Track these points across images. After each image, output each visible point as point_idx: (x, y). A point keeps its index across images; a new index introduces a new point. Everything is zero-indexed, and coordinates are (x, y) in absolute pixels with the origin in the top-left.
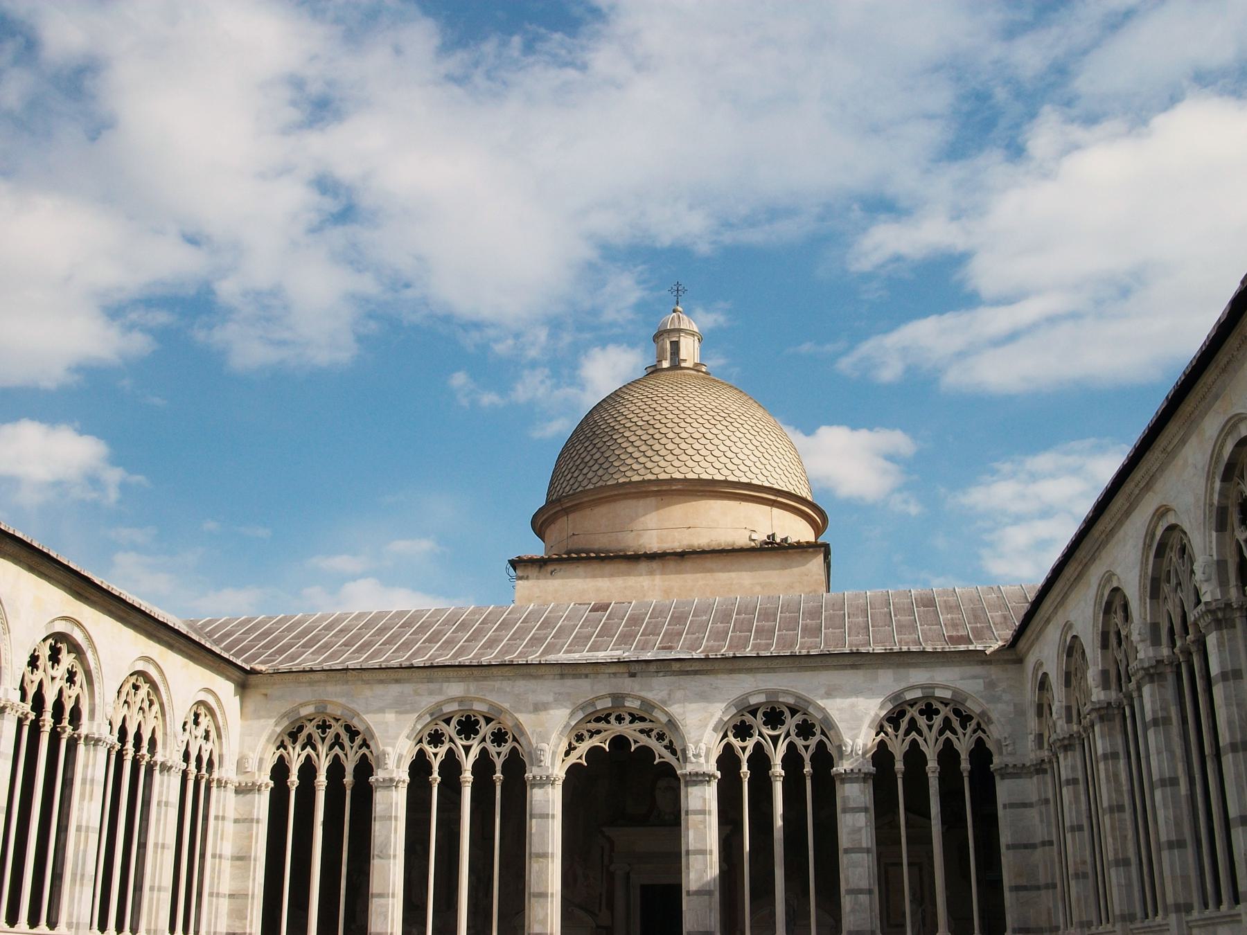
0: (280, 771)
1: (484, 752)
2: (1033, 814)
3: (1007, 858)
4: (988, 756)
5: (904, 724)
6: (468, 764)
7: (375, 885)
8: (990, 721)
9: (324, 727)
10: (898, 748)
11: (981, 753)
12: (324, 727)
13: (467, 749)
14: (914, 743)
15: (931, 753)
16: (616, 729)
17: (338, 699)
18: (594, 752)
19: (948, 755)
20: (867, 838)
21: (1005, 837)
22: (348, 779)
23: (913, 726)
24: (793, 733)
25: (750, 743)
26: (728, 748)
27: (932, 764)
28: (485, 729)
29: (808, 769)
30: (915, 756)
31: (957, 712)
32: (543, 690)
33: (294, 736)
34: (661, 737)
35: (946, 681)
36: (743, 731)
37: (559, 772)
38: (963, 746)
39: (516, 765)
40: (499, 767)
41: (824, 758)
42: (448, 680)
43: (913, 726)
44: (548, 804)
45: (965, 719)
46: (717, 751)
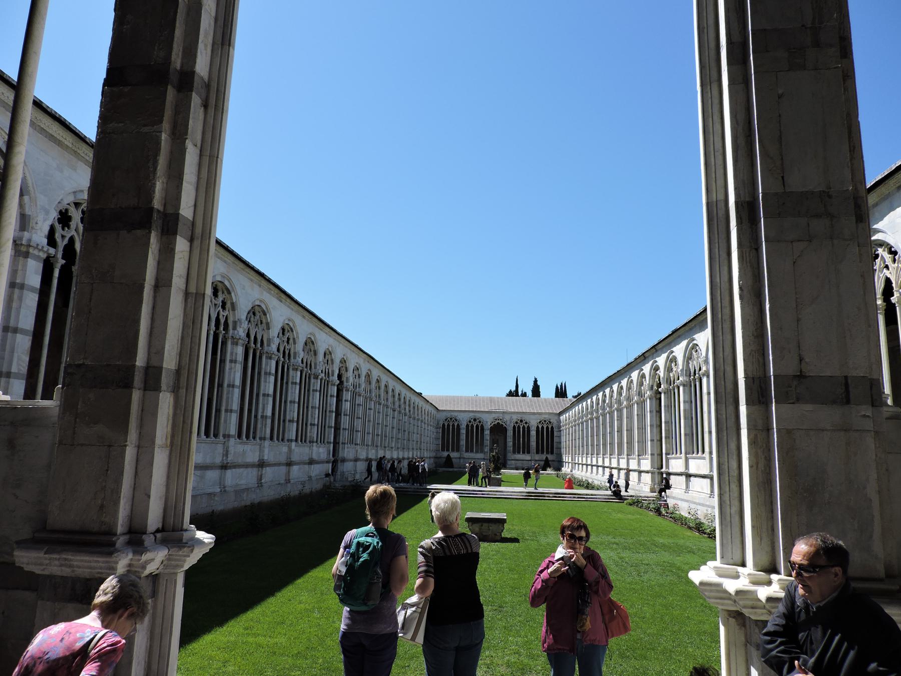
0: (444, 425)
11: (552, 428)
19: (547, 428)
30: (543, 428)
39: (482, 426)
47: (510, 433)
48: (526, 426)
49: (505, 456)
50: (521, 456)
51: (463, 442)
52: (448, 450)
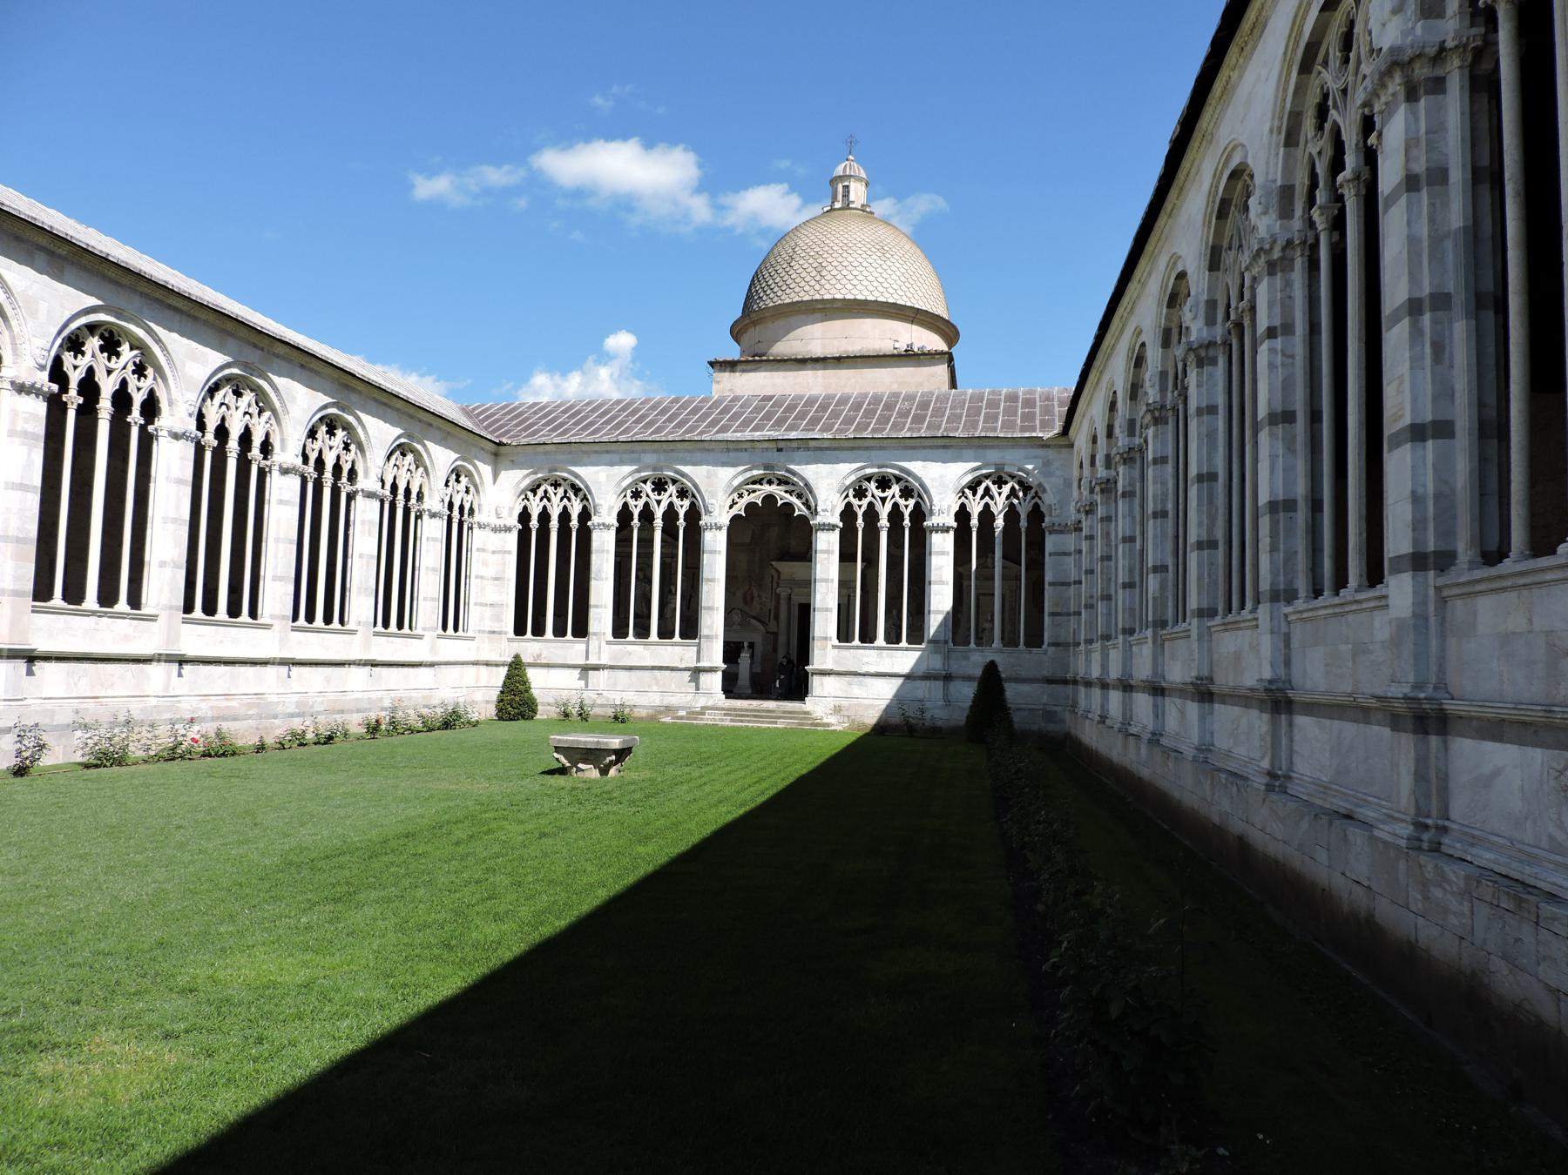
0: (524, 517)
1: (671, 505)
2: (1071, 560)
4: (1042, 517)
5: (981, 491)
6: (659, 513)
8: (1044, 491)
10: (975, 508)
11: (1036, 514)
13: (659, 502)
14: (987, 506)
18: (750, 507)
21: (1048, 578)
22: (574, 523)
23: (987, 491)
24: (898, 494)
25: (865, 502)
26: (849, 506)
28: (672, 489)
29: (907, 522)
31: (1020, 483)
33: (534, 491)
34: (799, 496)
37: (725, 520)
39: (694, 515)
40: (681, 516)
41: (919, 514)
42: (644, 452)
43: (987, 491)
44: (715, 545)
46: (841, 507)
47: (827, 545)
49: (804, 654)
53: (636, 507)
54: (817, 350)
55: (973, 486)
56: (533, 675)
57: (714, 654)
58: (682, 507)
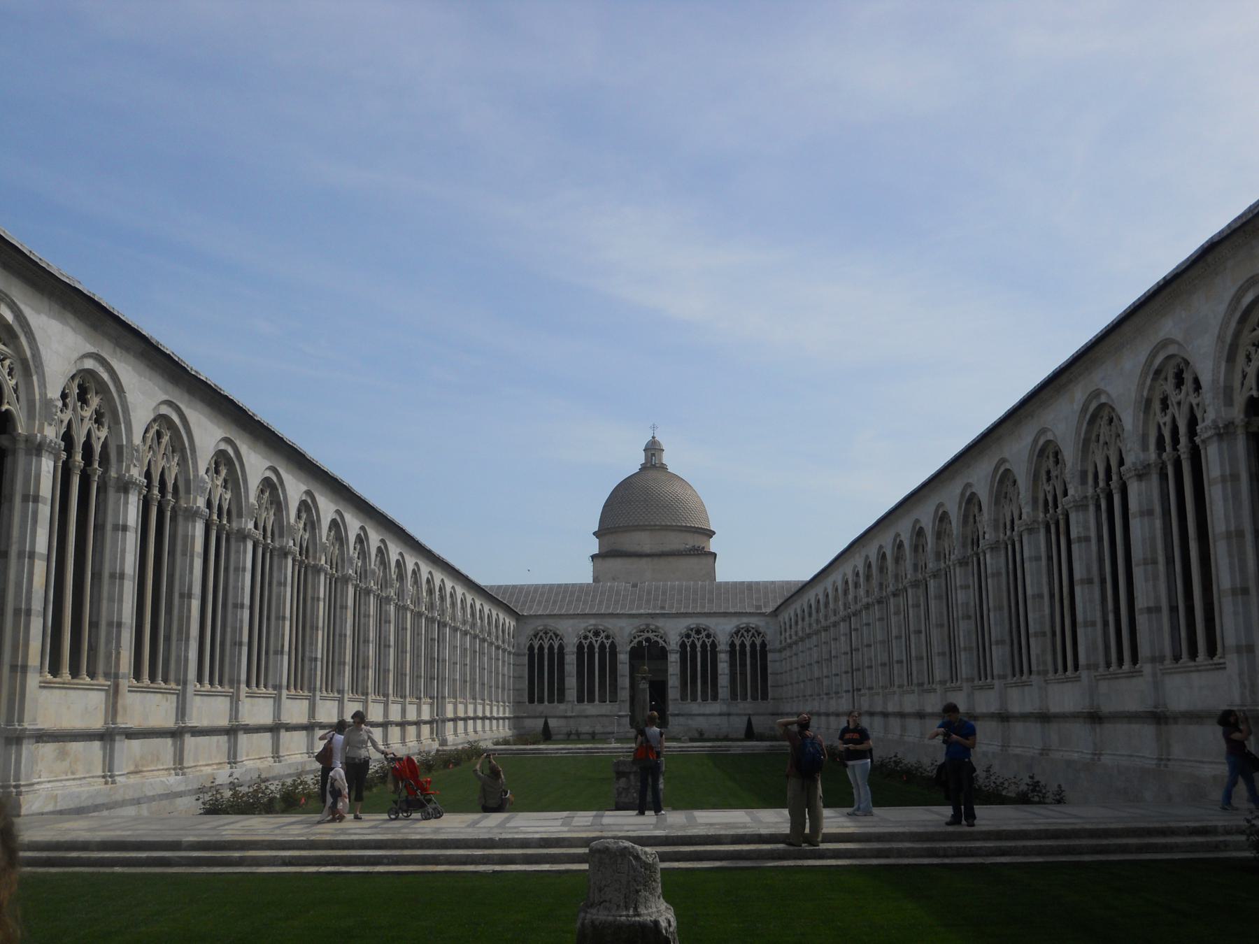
0: (531, 648)
3: (770, 677)
6: (597, 646)
7: (567, 685)
9: (546, 633)
10: (737, 642)
11: (763, 645)
12: (546, 633)
15: (748, 644)
16: (646, 635)
17: (552, 624)
18: (640, 643)
19: (753, 645)
20: (727, 671)
27: (748, 648)
28: (603, 635)
30: (743, 645)
32: (623, 623)
35: (754, 622)
36: (688, 636)
37: (628, 649)
38: (758, 642)
39: (613, 646)
41: (714, 645)
45: (759, 634)
47: (674, 658)
48: (708, 642)
50: (695, 708)
51: (571, 682)
52: (541, 701)
53: (586, 643)
54: (647, 548)
55: (737, 633)
56: (550, 721)
57: (626, 711)
58: (608, 643)
